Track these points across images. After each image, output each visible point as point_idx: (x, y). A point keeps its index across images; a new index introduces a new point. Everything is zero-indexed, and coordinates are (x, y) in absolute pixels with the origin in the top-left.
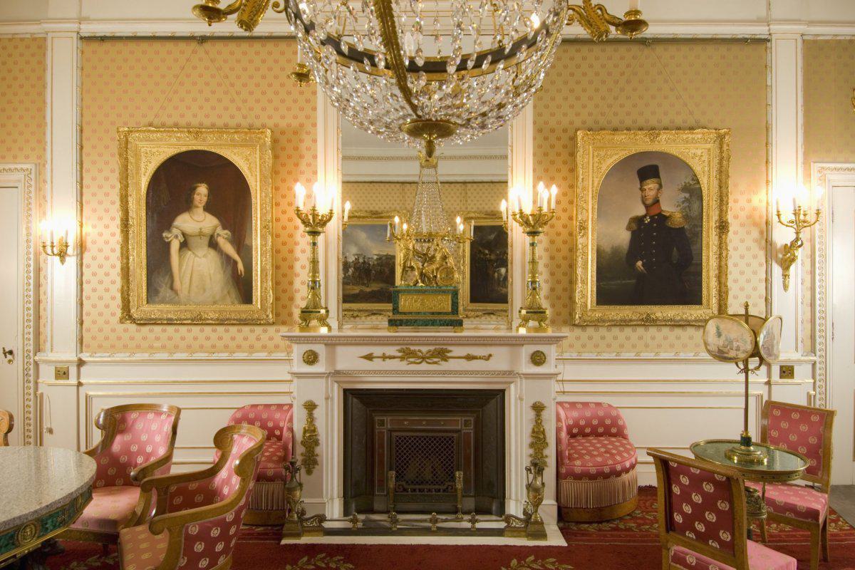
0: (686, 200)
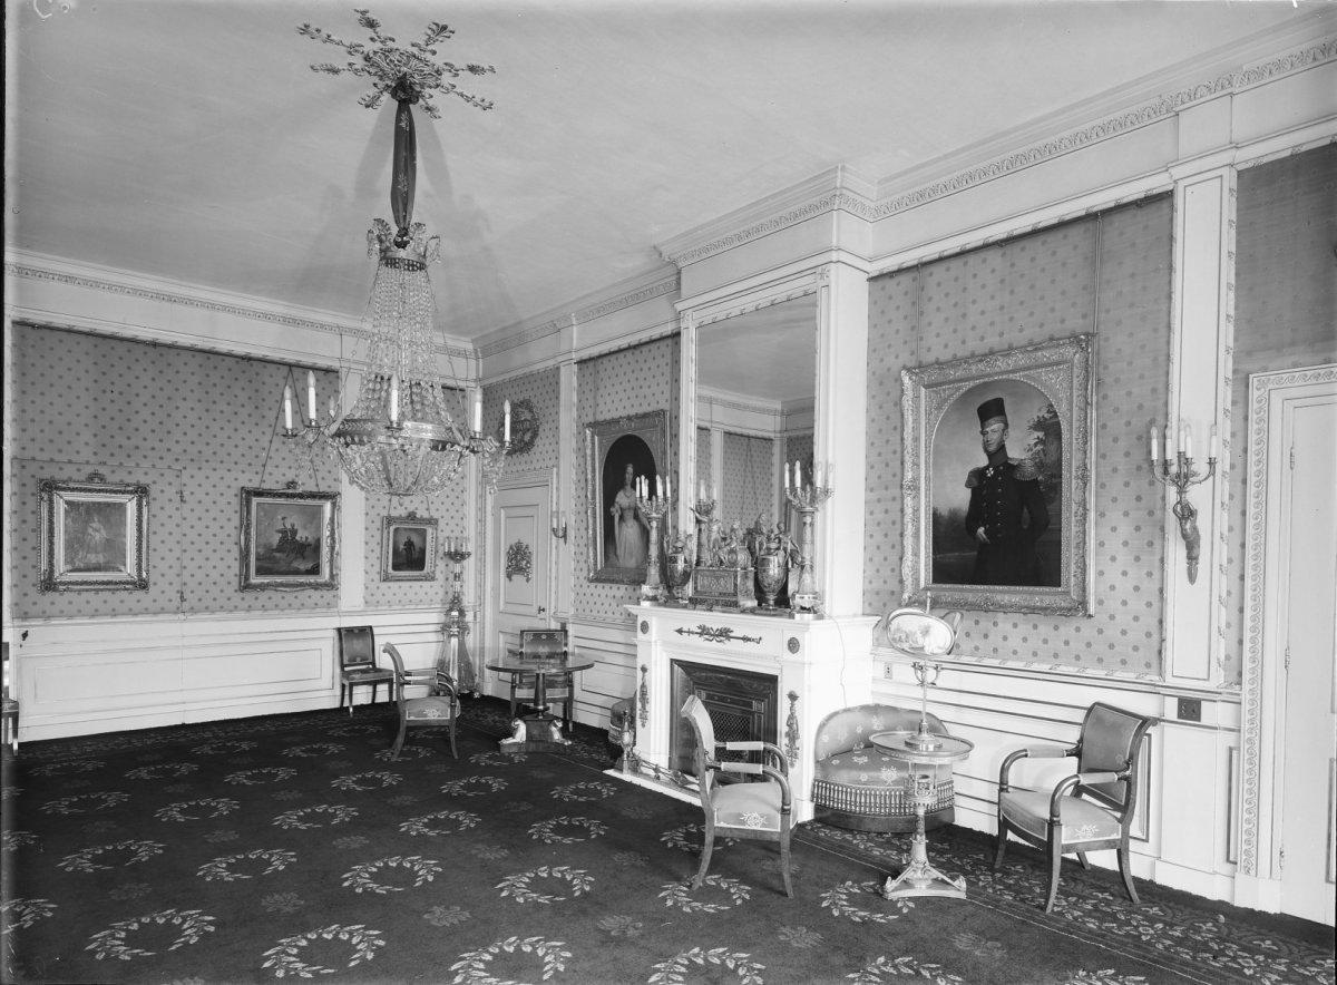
0: (1040, 441)
